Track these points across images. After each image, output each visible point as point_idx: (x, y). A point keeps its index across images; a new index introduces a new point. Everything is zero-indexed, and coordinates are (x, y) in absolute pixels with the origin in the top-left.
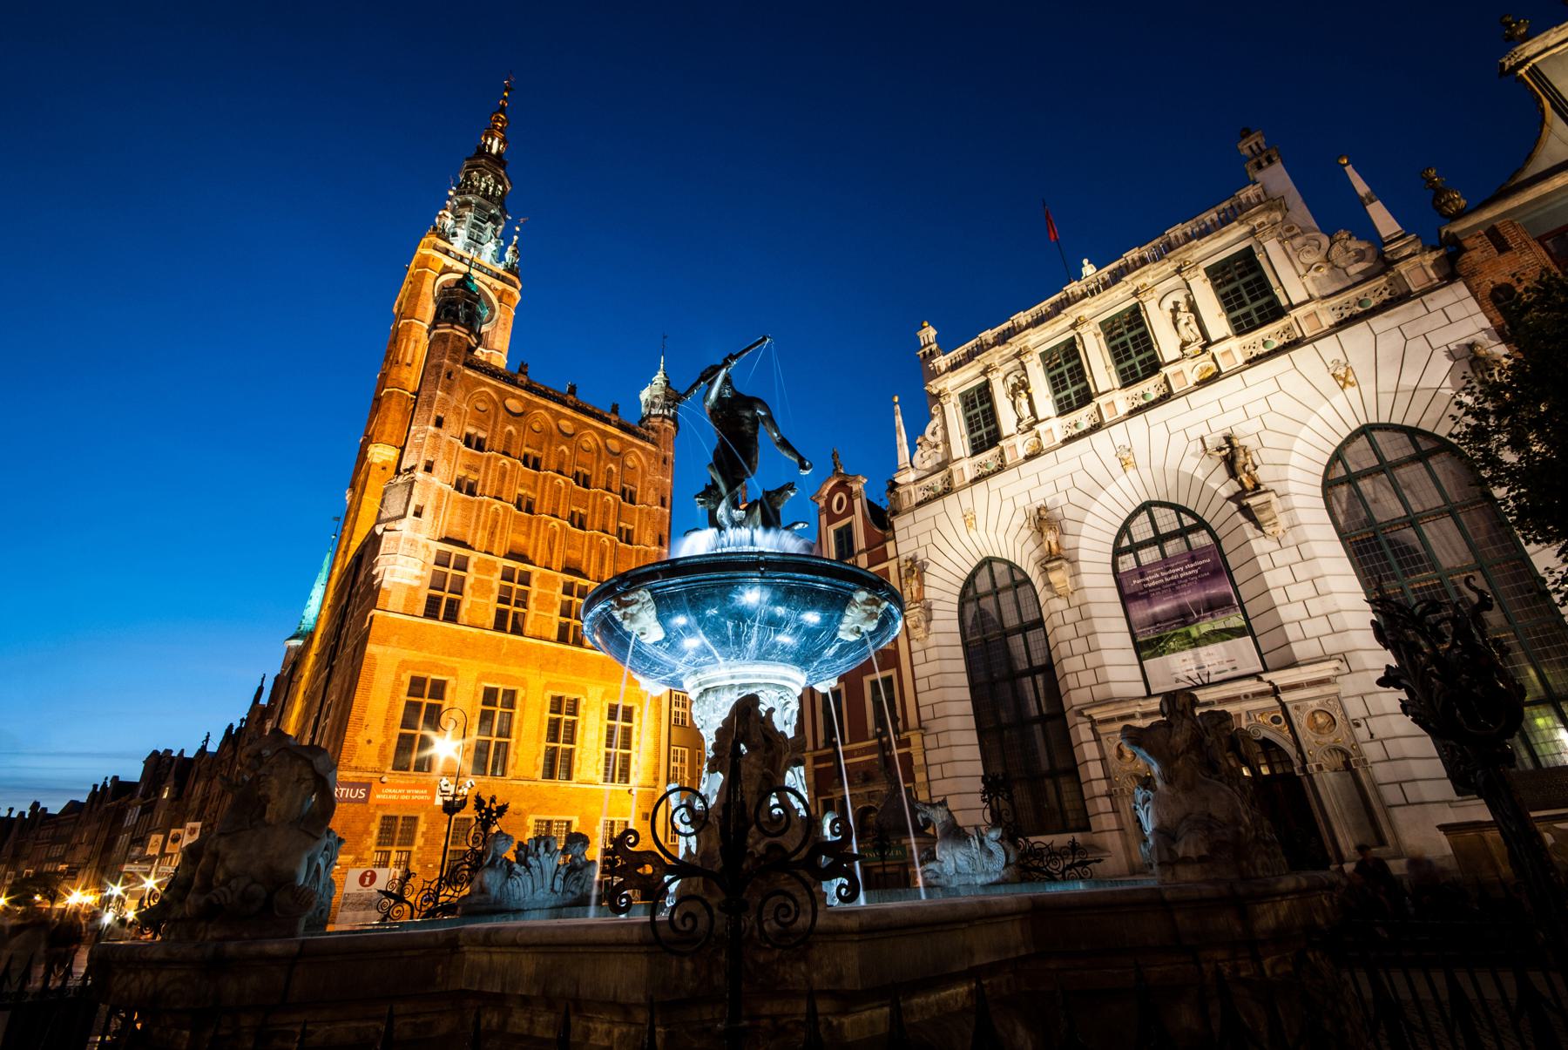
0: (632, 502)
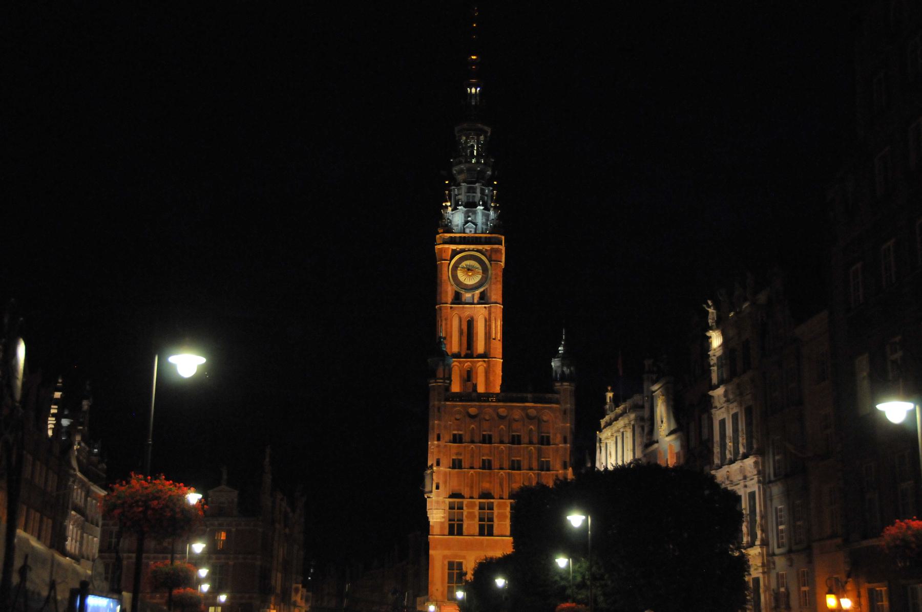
0: (548, 443)
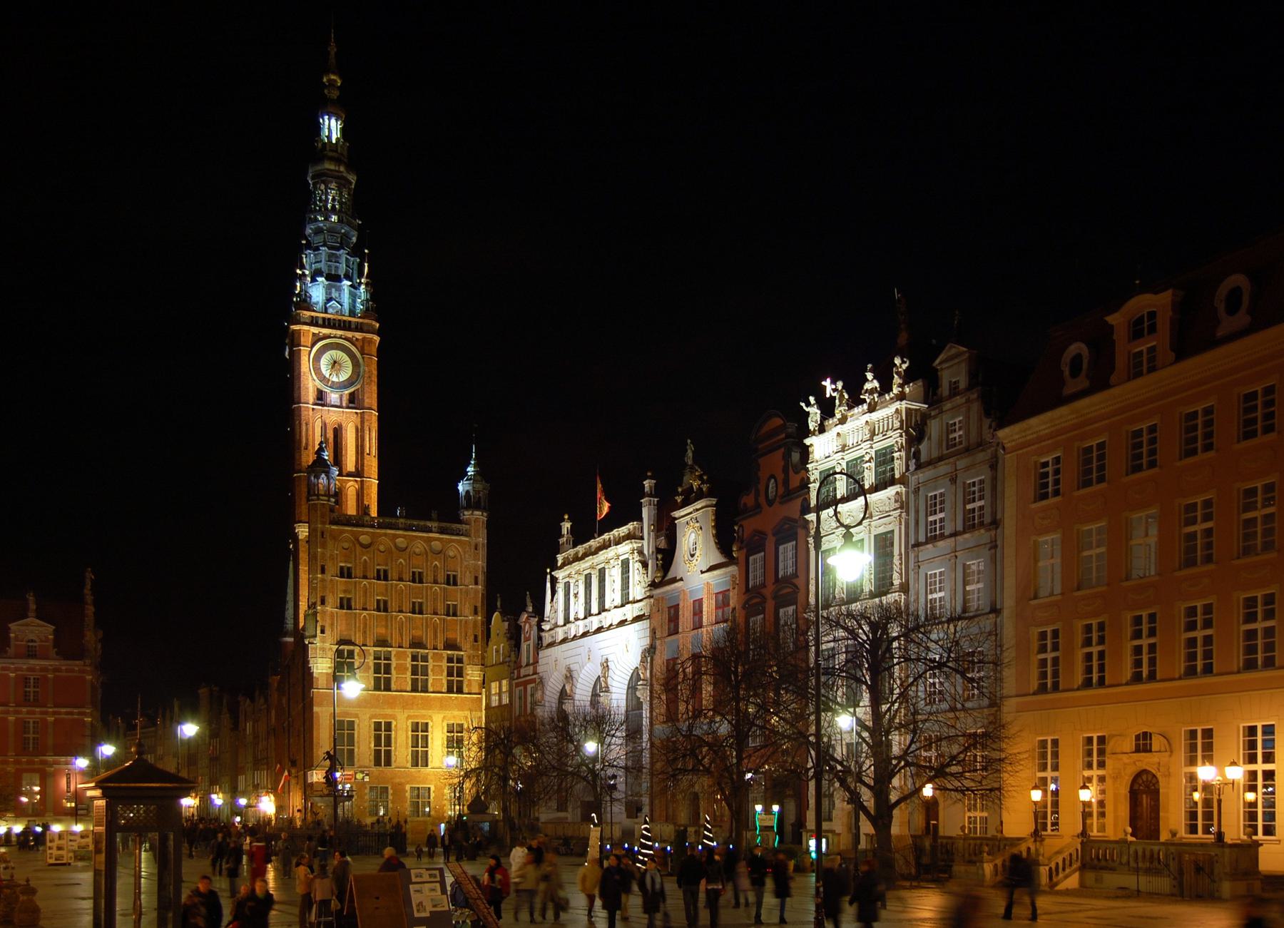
0: (455, 584)
